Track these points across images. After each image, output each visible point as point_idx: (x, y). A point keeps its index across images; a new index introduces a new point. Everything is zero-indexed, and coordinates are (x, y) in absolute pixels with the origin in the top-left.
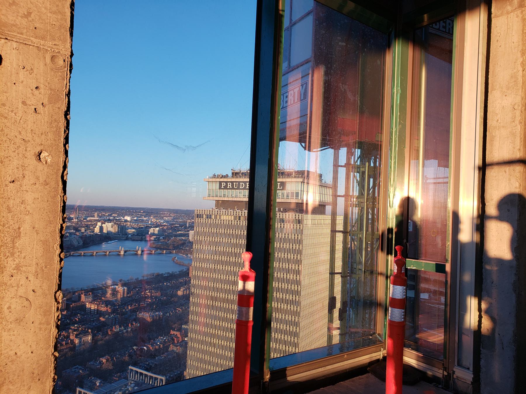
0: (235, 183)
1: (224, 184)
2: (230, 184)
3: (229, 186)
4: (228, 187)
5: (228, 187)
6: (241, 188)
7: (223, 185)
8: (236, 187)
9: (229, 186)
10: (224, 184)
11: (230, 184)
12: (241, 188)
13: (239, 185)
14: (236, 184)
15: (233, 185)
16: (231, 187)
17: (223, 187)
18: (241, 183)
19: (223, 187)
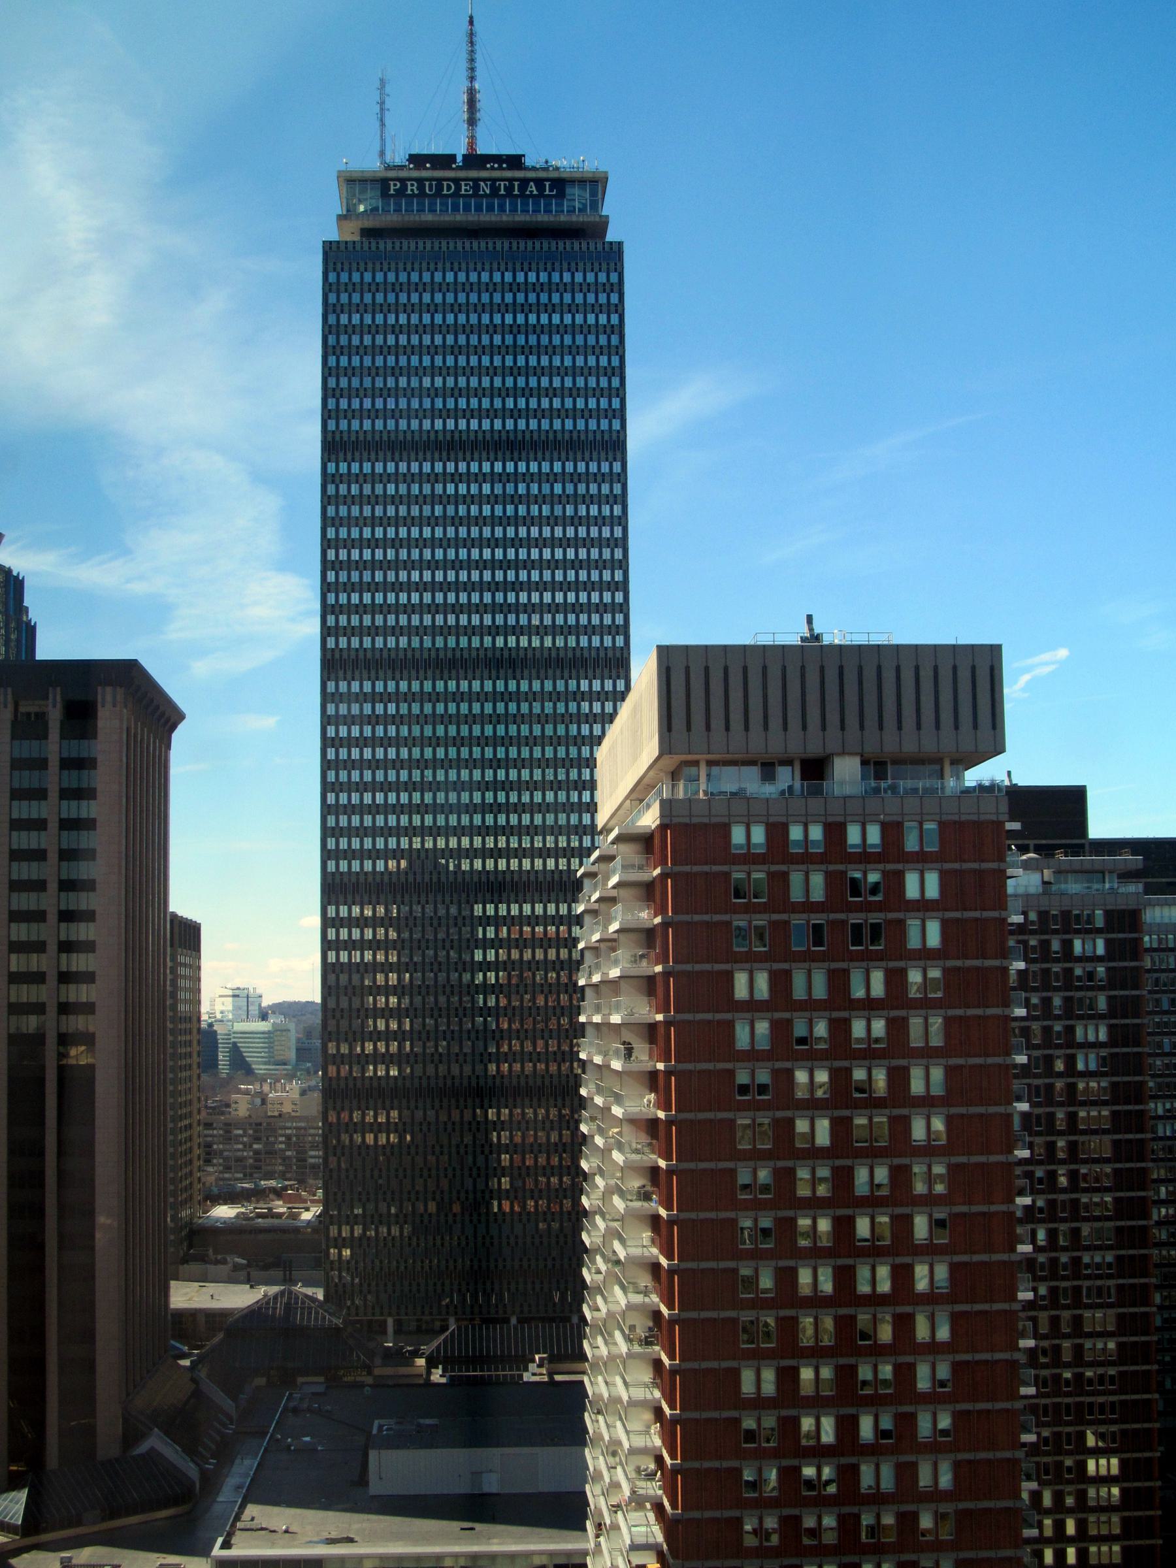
0: (427, 183)
4: (409, 192)
5: (409, 192)
6: (445, 192)
7: (392, 187)
8: (431, 190)
12: (445, 192)
13: (440, 188)
15: (421, 187)
16: (416, 192)
18: (445, 183)
19: (392, 192)
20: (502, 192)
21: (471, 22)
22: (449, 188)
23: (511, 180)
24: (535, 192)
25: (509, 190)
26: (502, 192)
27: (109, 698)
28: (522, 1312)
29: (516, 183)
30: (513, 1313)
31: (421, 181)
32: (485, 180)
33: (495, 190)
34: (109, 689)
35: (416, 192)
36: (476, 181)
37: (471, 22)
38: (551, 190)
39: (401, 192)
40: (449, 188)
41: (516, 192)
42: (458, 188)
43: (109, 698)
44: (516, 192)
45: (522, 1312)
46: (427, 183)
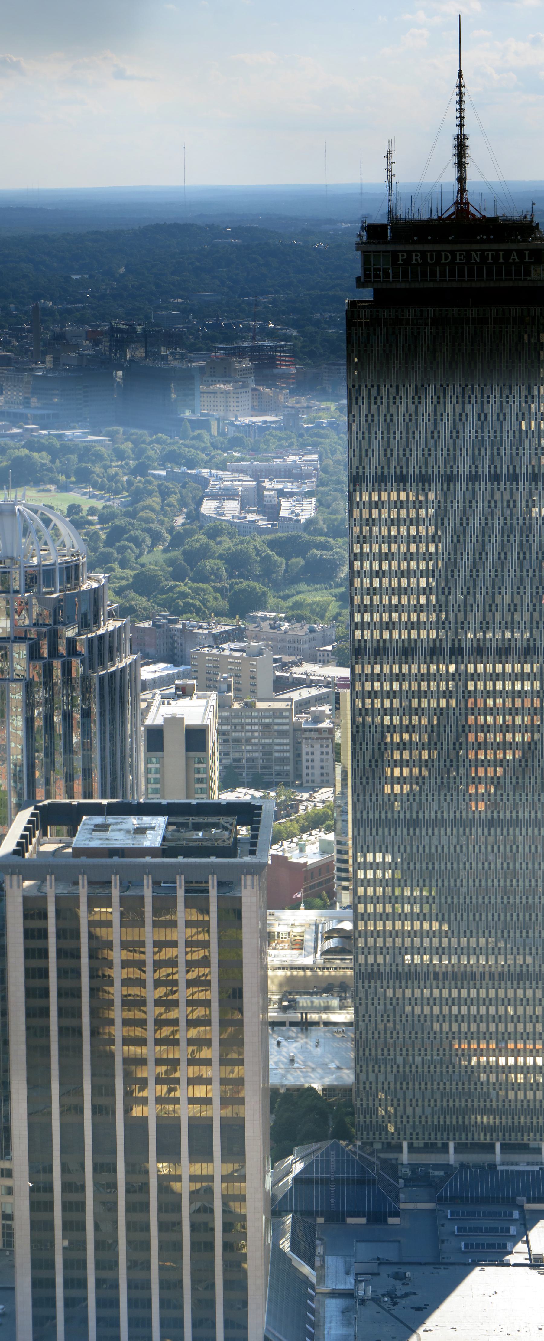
0: (429, 254)
1: (403, 256)
2: (417, 256)
3: (417, 260)
4: (414, 262)
5: (414, 262)
8: (431, 260)
9: (417, 260)
10: (403, 256)
11: (417, 256)
14: (432, 256)
15: (424, 257)
16: (420, 261)
17: (400, 262)
19: (400, 262)
20: (490, 261)
21: (460, 76)
22: (446, 258)
23: (497, 251)
24: (517, 260)
25: (496, 258)
26: (490, 261)
27: (249, 882)
28: (504, 1139)
29: (501, 253)
30: (498, 1140)
31: (423, 253)
32: (475, 251)
33: (484, 258)
34: (249, 878)
35: (420, 261)
36: (468, 252)
37: (460, 76)
38: (530, 258)
39: (408, 261)
40: (446, 258)
41: (501, 260)
42: (454, 258)
43: (249, 882)
44: (501, 260)
45: (504, 1139)
46: (429, 254)
